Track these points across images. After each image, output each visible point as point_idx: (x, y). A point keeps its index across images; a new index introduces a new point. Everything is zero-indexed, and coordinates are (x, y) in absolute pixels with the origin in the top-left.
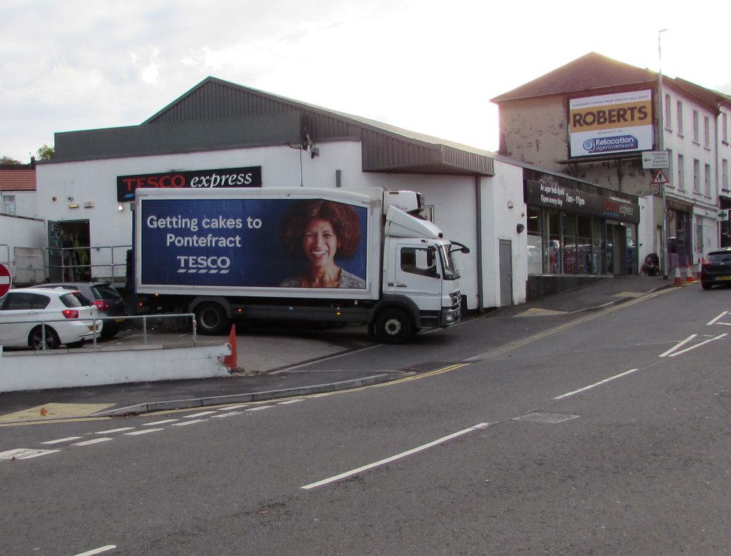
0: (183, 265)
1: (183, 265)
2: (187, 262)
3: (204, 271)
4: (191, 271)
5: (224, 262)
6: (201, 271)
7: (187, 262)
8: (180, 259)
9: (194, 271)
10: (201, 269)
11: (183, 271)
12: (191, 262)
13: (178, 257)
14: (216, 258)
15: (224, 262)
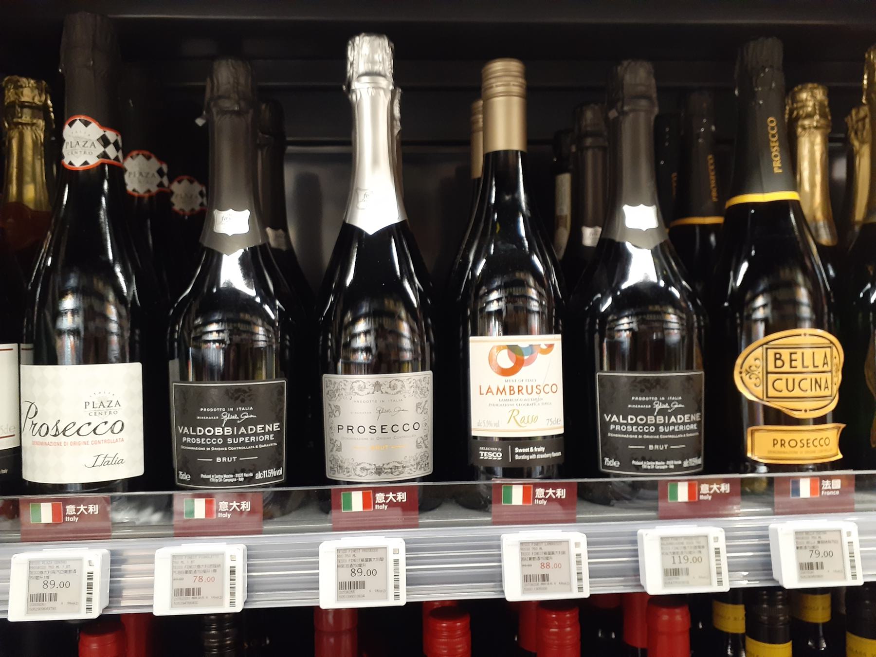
0: (482, 455)
1: (482, 455)
2: (483, 454)
3: (491, 458)
4: (485, 458)
5: (499, 455)
6: (489, 458)
7: (483, 454)
8: (480, 454)
9: (487, 458)
10: (489, 457)
11: (482, 458)
12: (485, 455)
13: (480, 452)
14: (496, 453)
15: (499, 455)
